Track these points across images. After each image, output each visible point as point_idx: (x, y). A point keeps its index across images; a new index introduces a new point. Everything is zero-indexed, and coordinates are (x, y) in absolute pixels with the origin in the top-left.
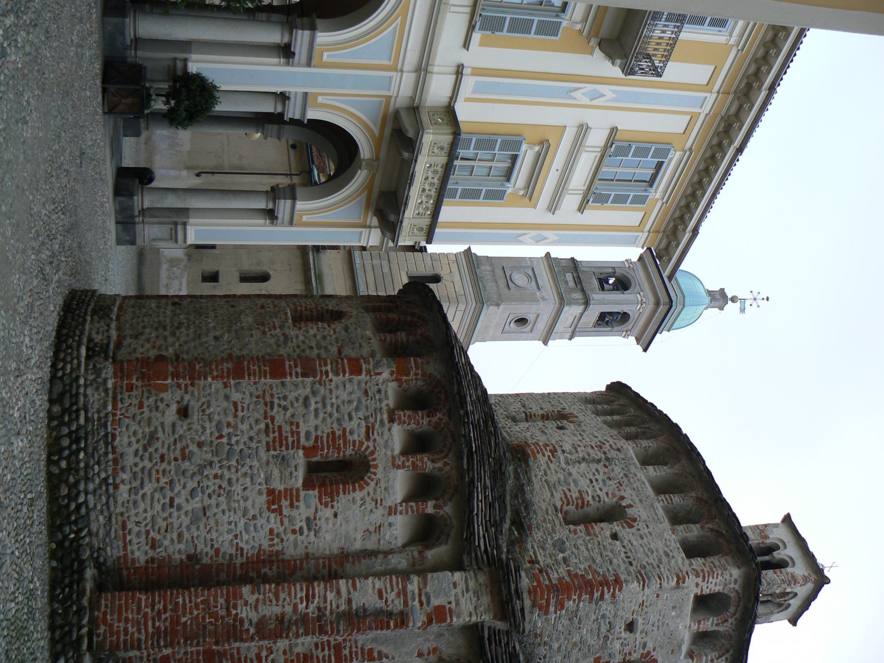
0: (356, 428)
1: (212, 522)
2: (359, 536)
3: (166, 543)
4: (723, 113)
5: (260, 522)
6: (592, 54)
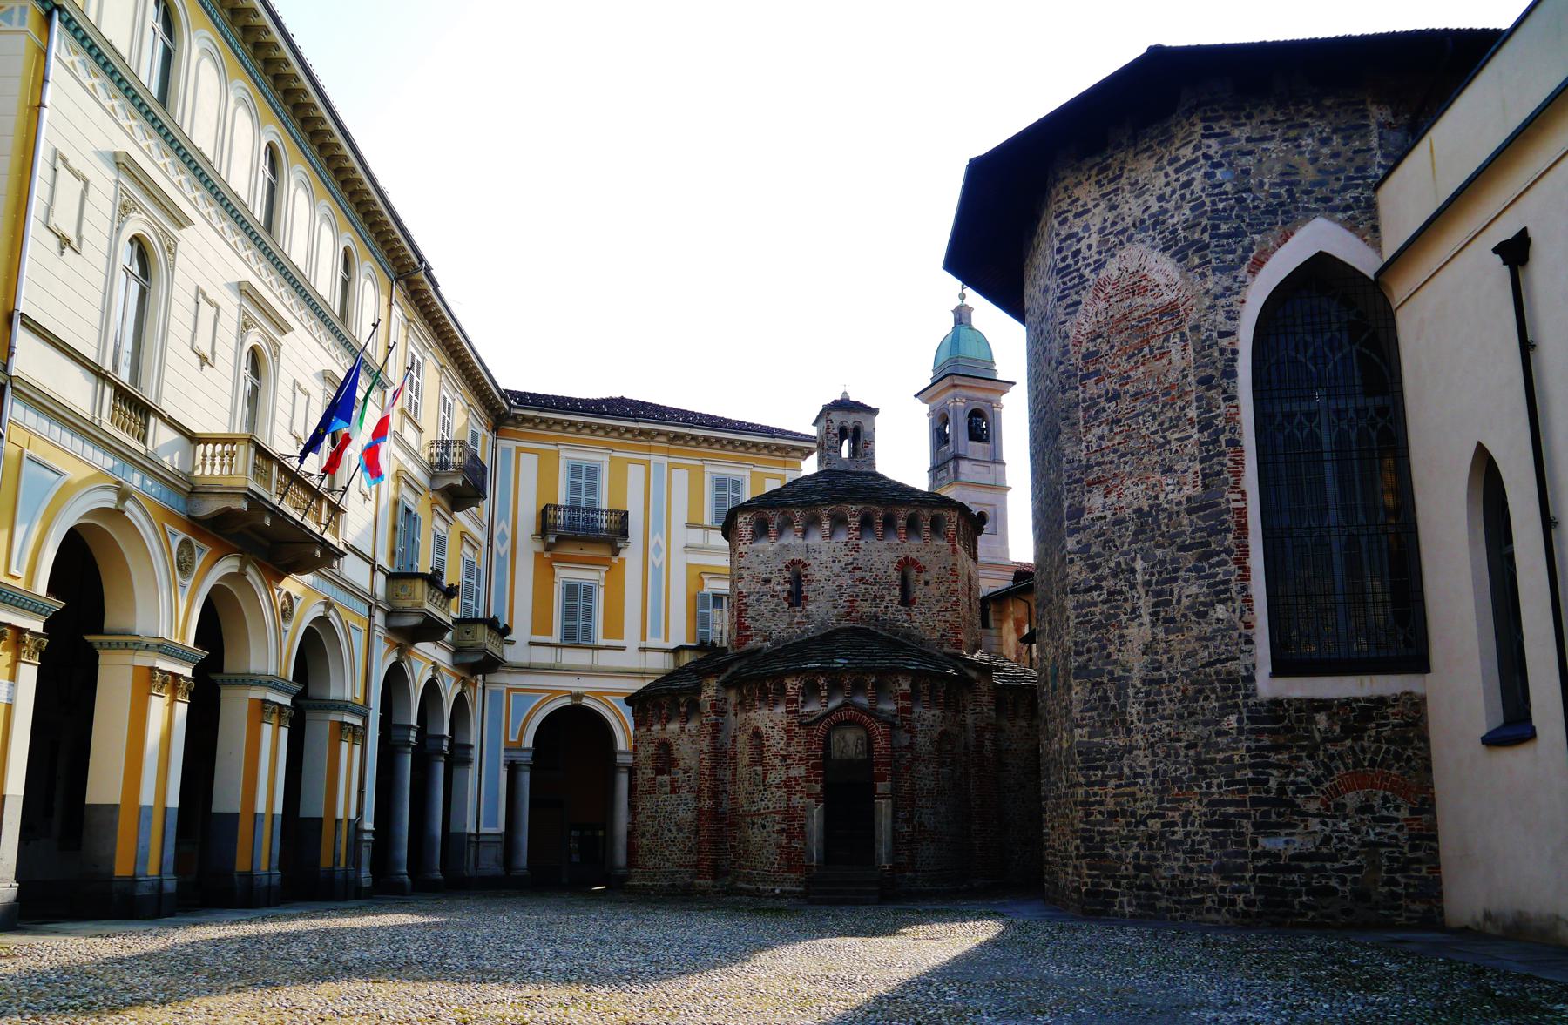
0: (651, 748)
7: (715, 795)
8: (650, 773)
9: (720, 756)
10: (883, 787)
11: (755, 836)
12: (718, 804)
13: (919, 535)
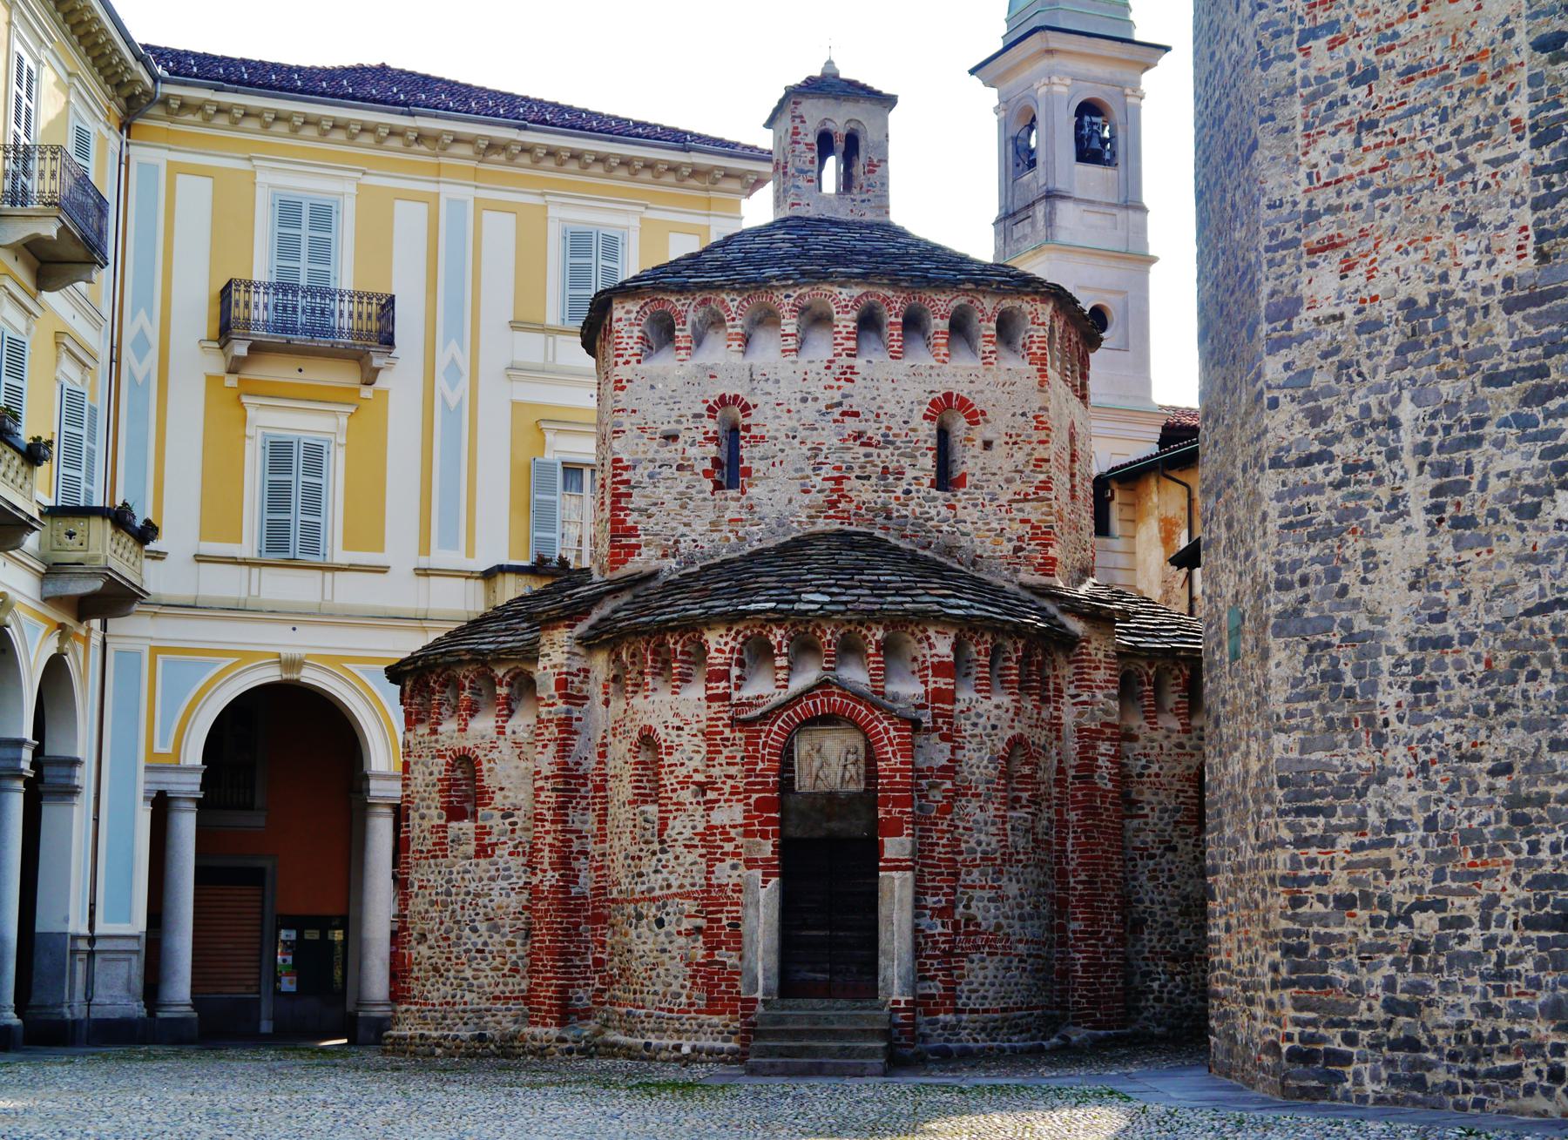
1: (500, 912)
2: (523, 764)
3: (514, 957)
4: (473, 164)
5: (501, 865)
6: (385, 393)
7: (564, 861)
8: (435, 816)
9: (573, 785)
10: (895, 847)
11: (643, 941)
12: (570, 878)
13: (973, 348)
